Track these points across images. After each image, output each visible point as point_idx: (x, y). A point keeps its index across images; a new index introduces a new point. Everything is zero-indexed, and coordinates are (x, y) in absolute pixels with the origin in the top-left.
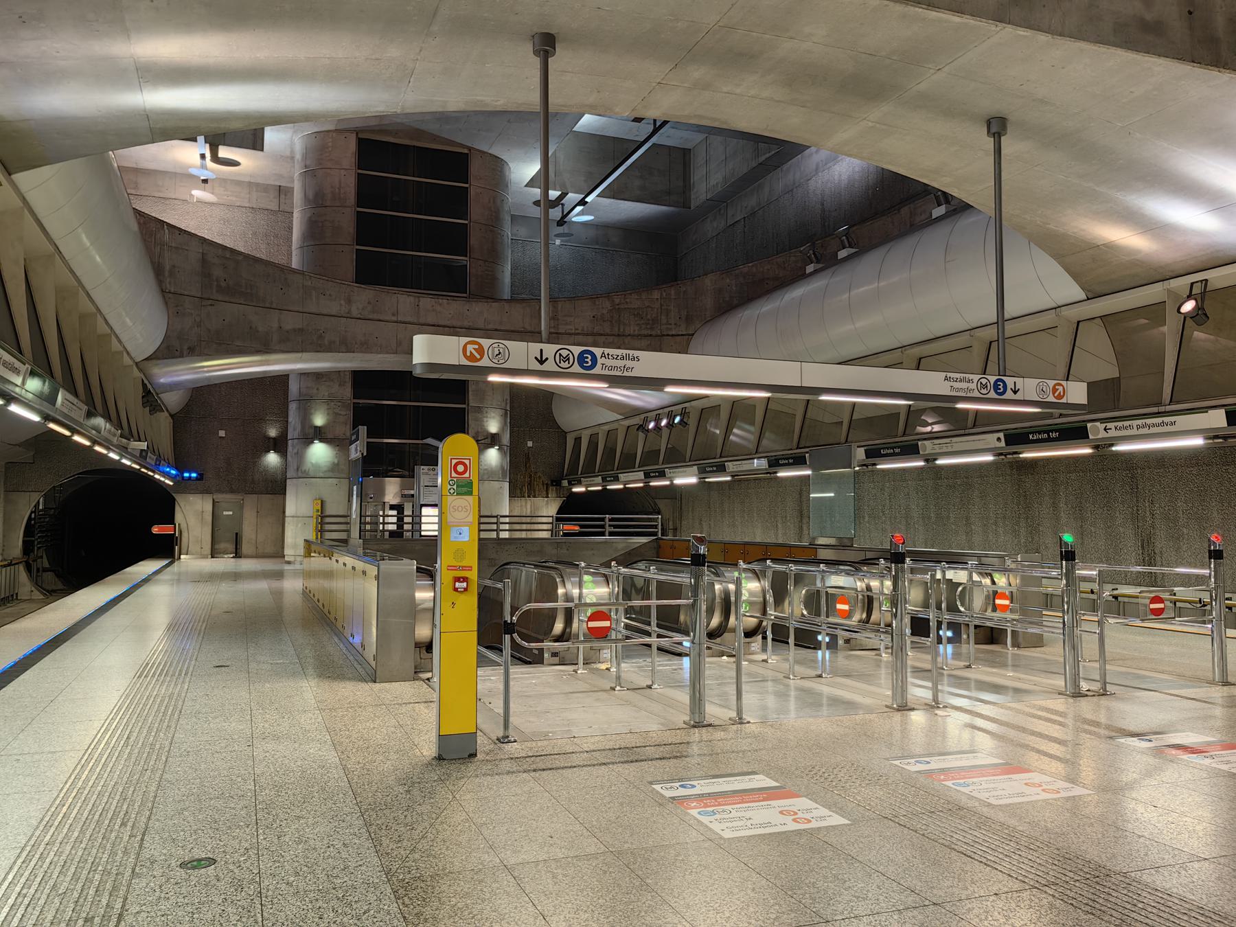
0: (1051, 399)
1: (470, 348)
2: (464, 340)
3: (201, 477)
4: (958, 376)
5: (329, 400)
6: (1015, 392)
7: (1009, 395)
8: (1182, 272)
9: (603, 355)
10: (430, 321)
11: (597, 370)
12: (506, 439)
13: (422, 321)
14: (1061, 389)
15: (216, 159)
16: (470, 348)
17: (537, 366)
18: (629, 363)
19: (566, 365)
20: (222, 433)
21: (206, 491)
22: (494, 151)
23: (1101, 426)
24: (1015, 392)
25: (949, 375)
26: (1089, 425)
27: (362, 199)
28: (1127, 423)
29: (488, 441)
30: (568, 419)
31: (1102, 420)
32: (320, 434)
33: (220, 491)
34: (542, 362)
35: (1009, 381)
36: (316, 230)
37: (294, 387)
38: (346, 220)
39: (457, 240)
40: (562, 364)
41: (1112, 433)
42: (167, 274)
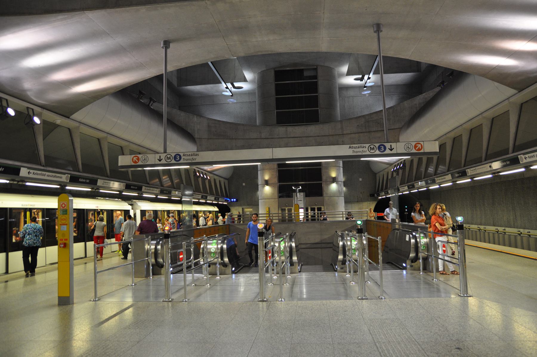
0: (414, 151)
1: (135, 158)
2: (133, 156)
3: (237, 201)
4: (357, 145)
5: (270, 169)
6: (391, 150)
7: (388, 151)
9: (184, 155)
10: (292, 136)
12: (342, 178)
13: (288, 136)
14: (420, 146)
15: (234, 87)
16: (135, 158)
17: (159, 163)
18: (194, 157)
19: (169, 160)
20: (244, 184)
21: (240, 205)
23: (523, 156)
24: (391, 150)
25: (351, 146)
26: (519, 156)
27: (277, 93)
28: (532, 154)
29: (332, 180)
31: (524, 154)
32: (267, 183)
33: (244, 205)
34: (160, 160)
35: (388, 145)
36: (264, 107)
37: (259, 167)
38: (272, 102)
39: (315, 102)
40: (168, 161)
41: (528, 160)
42: (196, 132)
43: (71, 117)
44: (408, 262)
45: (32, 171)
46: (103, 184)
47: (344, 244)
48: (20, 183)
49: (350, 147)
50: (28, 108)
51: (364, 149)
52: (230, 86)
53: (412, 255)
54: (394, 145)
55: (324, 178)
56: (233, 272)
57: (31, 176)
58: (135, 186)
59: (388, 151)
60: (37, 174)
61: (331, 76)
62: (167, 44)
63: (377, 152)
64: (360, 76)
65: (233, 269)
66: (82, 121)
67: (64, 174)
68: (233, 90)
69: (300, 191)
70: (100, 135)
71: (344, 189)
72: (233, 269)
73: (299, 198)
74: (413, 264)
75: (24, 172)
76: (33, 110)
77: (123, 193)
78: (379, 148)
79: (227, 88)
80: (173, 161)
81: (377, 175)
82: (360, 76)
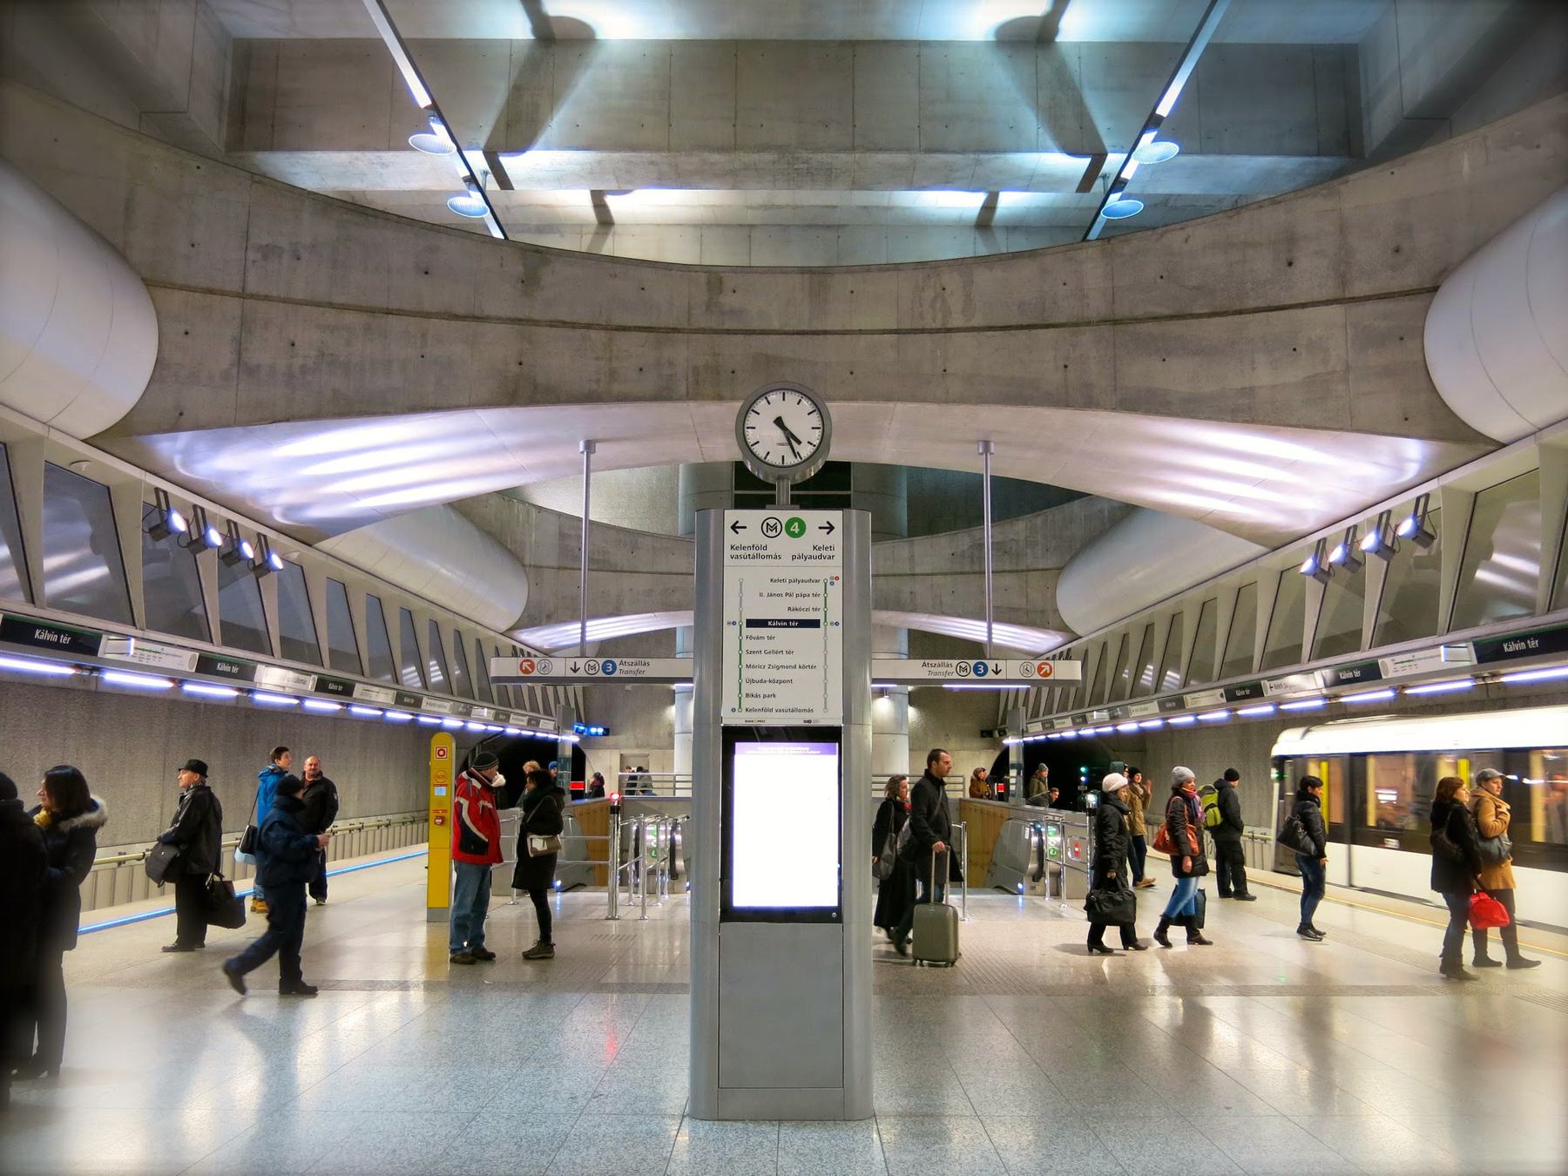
0: (1037, 676)
7: (990, 675)
34: (575, 671)
35: (991, 664)
43: (321, 545)
44: (1027, 880)
51: (950, 670)
53: (1033, 866)
54: (1001, 664)
59: (990, 675)
62: (590, 446)
63: (973, 676)
67: (308, 673)
71: (912, 712)
78: (976, 669)
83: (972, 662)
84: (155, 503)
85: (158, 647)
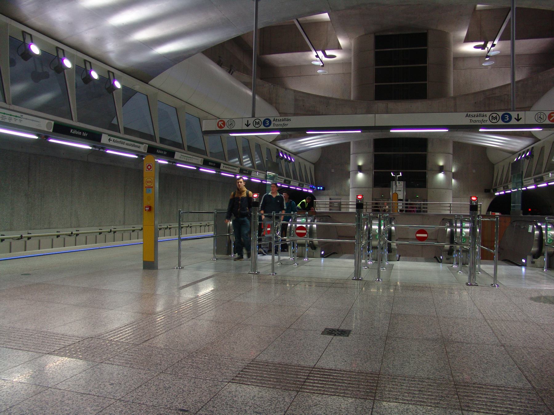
1: (220, 123)
3: (324, 189)
4: (476, 113)
7: (513, 122)
8: (113, 65)
9: (274, 120)
11: (271, 127)
15: (326, 56)
16: (220, 123)
18: (286, 122)
19: (258, 126)
22: (441, 28)
25: (469, 113)
30: (492, 157)
32: (360, 169)
34: (248, 125)
35: (514, 114)
39: (422, 74)
43: (151, 82)
44: (529, 258)
45: (112, 138)
46: (180, 157)
47: (452, 231)
48: (101, 150)
49: (467, 116)
50: (109, 72)
51: (485, 118)
52: (320, 53)
53: (534, 249)
54: (522, 114)
55: (429, 166)
56: (322, 256)
57: (111, 143)
58: (213, 162)
59: (513, 122)
60: (117, 142)
61: (444, 44)
63: (501, 122)
64: (482, 43)
65: (323, 253)
66: (160, 88)
67: (142, 143)
68: (325, 59)
69: (400, 179)
70: (178, 103)
72: (323, 253)
73: (399, 189)
74: (535, 260)
75: (105, 139)
76: (113, 73)
77: (201, 170)
78: (503, 118)
79: (317, 56)
80: (262, 127)
81: (496, 167)
82: (482, 43)
83: (501, 114)
84: (56, 55)
85: (19, 115)
